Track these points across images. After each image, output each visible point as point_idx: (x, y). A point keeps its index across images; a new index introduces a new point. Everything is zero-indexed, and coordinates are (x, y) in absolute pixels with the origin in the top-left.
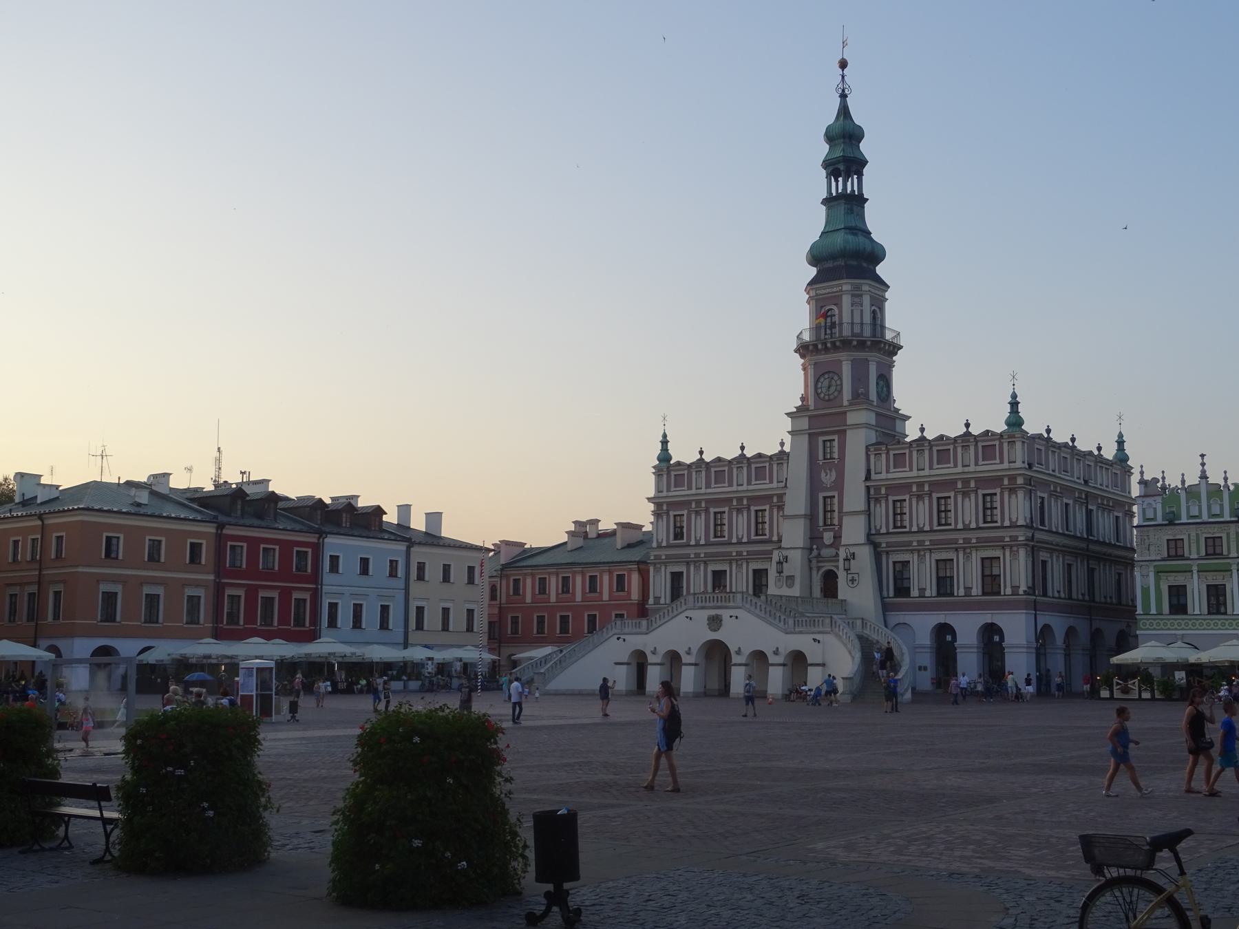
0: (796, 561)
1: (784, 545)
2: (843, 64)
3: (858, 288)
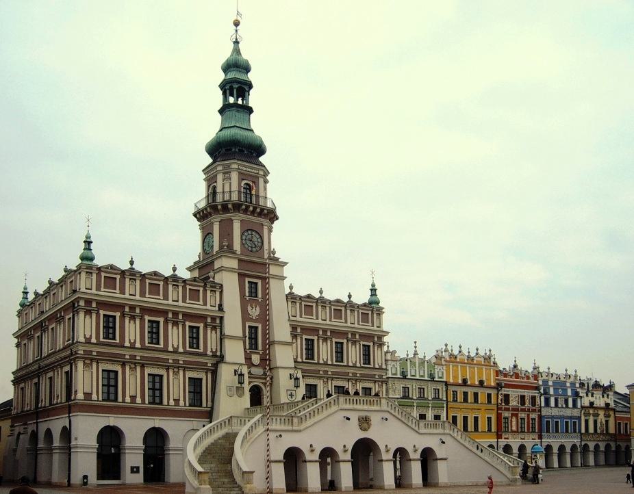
1: (228, 358)
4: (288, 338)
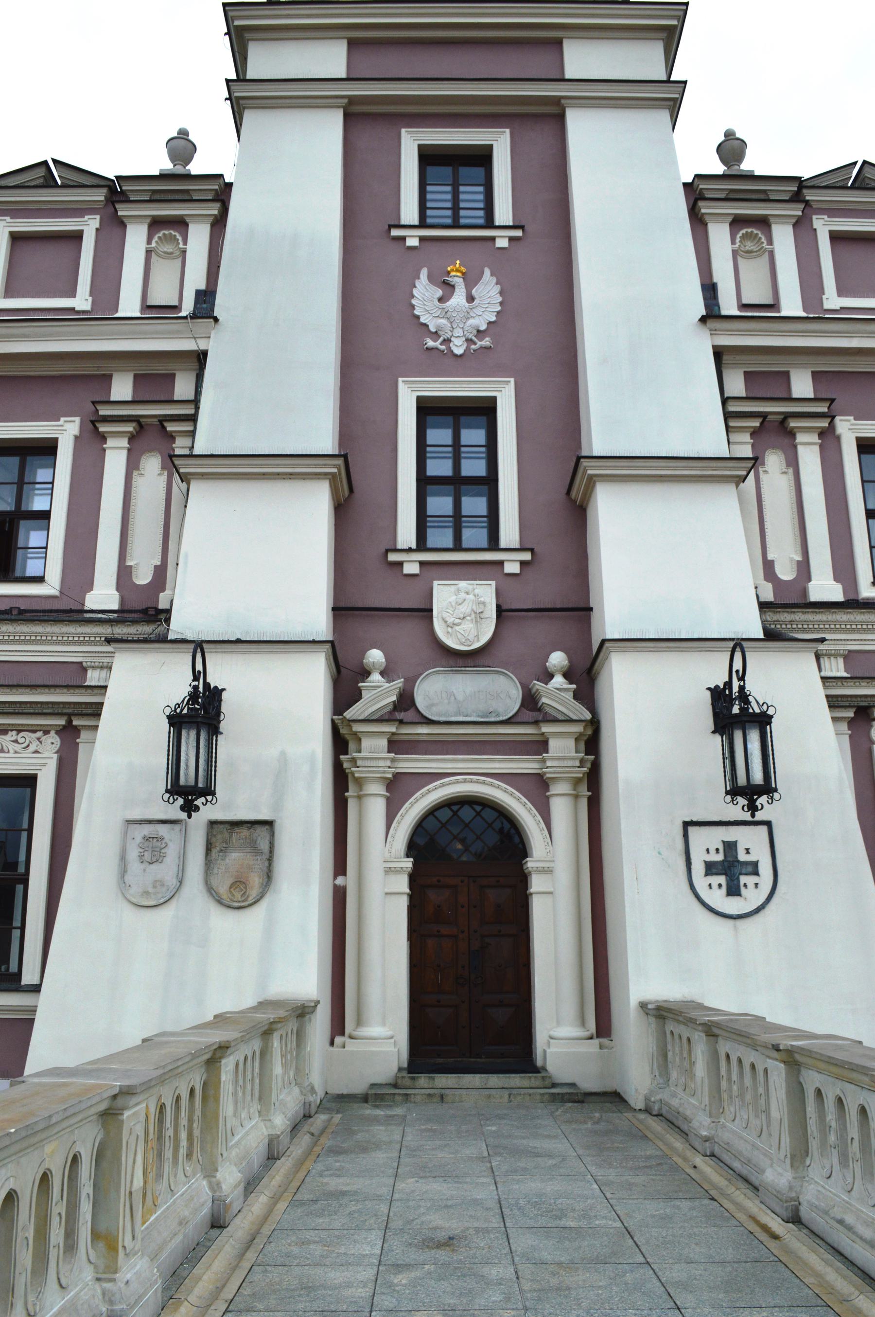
0: (281, 716)
4: (708, 435)
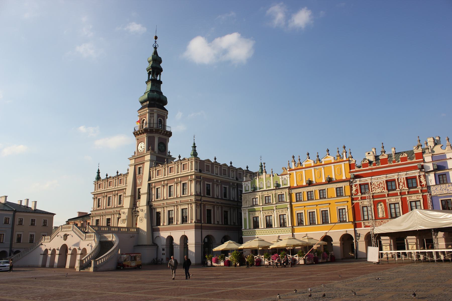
1: (124, 208)
2: (156, 38)
3: (153, 111)
